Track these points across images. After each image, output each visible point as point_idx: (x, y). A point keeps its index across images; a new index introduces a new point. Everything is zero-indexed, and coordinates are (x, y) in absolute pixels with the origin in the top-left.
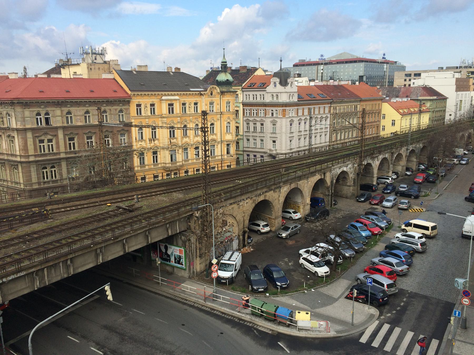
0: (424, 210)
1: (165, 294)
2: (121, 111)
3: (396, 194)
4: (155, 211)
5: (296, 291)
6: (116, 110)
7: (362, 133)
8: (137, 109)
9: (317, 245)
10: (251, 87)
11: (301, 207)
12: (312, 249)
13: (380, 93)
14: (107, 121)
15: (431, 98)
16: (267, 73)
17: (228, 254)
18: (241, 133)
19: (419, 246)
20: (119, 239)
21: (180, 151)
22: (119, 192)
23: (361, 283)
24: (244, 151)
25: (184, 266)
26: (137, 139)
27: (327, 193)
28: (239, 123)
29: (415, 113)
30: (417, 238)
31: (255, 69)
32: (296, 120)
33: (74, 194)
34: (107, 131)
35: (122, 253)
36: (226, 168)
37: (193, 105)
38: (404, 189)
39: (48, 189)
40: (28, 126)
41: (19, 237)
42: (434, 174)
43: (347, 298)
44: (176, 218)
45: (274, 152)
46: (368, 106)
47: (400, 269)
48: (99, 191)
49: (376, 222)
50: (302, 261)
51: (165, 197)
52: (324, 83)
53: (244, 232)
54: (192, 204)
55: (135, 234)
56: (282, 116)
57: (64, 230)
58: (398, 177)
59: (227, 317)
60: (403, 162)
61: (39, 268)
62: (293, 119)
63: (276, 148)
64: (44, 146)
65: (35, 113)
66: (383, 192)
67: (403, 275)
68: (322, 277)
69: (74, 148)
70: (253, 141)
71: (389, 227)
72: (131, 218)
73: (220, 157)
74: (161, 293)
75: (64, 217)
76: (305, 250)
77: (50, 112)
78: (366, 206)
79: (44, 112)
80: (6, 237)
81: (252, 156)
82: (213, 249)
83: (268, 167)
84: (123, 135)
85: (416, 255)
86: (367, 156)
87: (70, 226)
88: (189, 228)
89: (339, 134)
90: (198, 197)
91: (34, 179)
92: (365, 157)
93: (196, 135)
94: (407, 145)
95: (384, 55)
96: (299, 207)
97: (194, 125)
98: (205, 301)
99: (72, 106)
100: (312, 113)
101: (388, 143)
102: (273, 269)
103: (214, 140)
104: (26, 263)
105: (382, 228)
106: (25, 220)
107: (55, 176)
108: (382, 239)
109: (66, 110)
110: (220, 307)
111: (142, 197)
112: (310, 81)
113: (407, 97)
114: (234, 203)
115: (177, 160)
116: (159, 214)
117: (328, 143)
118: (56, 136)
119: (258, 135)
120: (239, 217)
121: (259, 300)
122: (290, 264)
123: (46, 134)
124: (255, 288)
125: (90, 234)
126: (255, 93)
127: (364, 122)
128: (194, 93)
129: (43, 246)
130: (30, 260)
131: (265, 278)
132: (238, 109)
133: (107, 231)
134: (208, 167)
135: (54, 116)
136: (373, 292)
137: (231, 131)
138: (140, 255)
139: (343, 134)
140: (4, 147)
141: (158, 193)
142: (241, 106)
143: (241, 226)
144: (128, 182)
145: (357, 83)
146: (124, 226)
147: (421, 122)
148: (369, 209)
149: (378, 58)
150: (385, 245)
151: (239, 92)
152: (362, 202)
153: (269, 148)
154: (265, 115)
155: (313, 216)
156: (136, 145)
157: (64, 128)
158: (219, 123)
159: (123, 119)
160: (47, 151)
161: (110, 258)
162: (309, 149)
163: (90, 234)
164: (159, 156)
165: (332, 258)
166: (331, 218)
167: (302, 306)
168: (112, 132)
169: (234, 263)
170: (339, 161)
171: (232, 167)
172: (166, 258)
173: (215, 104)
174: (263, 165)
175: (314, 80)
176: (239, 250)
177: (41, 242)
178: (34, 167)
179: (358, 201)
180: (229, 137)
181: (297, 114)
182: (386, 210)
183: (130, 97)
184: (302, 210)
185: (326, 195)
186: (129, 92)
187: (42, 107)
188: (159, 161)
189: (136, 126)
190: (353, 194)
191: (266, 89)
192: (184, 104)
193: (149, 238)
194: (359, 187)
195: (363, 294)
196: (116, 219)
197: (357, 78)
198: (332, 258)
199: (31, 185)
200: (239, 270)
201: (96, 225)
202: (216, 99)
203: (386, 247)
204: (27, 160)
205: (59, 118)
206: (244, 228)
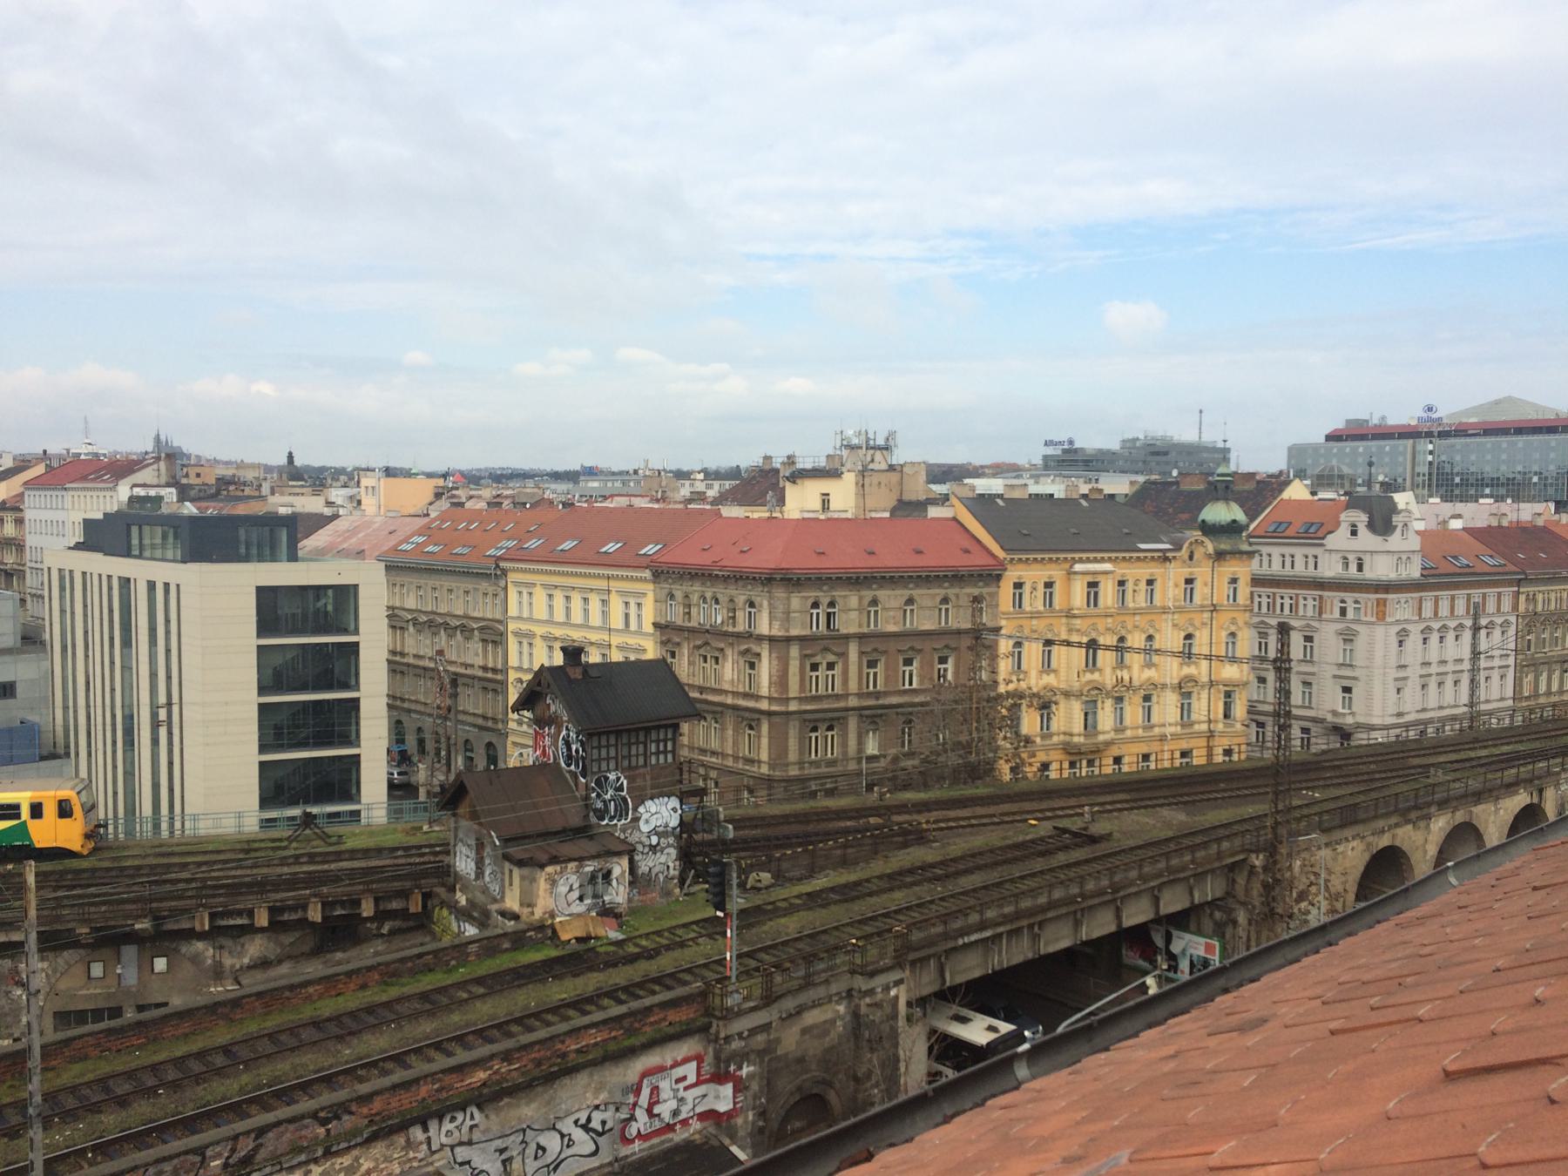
21: (1109, 703)
37: (1143, 586)
40: (794, 632)
45: (1349, 720)
56: (1374, 619)
62: (1409, 627)
63: (1354, 709)
65: (810, 602)
73: (1204, 727)
77: (838, 599)
89: (1545, 675)
91: (793, 756)
97: (1144, 637)
99: (881, 587)
109: (868, 595)
115: (1100, 727)
118: (843, 655)
123: (826, 649)
126: (1287, 550)
153: (1328, 707)
154: (1320, 614)
157: (861, 637)
181: (1420, 615)
187: (825, 588)
202: (1202, 572)
204: (783, 709)
205: (854, 615)
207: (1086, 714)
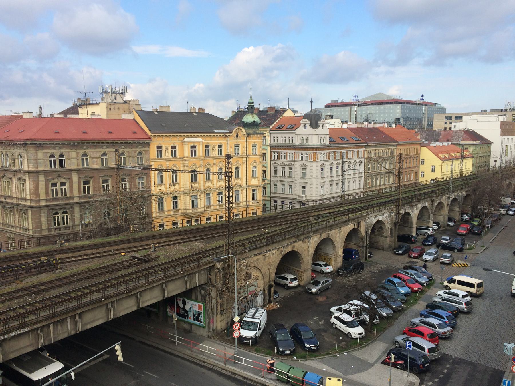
0: (469, 265)
1: (181, 355)
2: (140, 153)
3: (438, 247)
4: (173, 261)
5: (327, 354)
6: (135, 152)
7: (399, 179)
8: (157, 151)
9: (350, 302)
10: (280, 128)
11: (333, 259)
12: (345, 307)
13: (419, 137)
14: (124, 163)
15: (474, 142)
16: (297, 115)
17: (252, 311)
18: (268, 177)
19: (464, 306)
20: (133, 293)
21: (202, 196)
22: (135, 240)
23: (400, 346)
24: (271, 197)
25: (203, 324)
26: (157, 183)
27: (361, 245)
28: (266, 167)
29: (456, 158)
30: (461, 296)
31: (284, 110)
32: (327, 164)
33: (87, 242)
34: (124, 174)
35: (135, 308)
36: (251, 215)
37: (217, 148)
38: (446, 242)
39: (58, 236)
40: (41, 169)
41: (25, 289)
42: (479, 225)
43: (383, 363)
44: (196, 270)
45: (304, 198)
46: (405, 150)
47: (442, 331)
48: (113, 238)
49: (416, 278)
50: (333, 320)
51: (184, 246)
52: (359, 125)
53: (270, 287)
54: (213, 254)
55: (150, 287)
56: (312, 160)
57: (73, 282)
58: (439, 228)
59: (250, 382)
60: (445, 211)
61: (44, 323)
62: (324, 163)
64: (56, 190)
65: (49, 155)
66: (423, 244)
67: (447, 338)
68: (356, 339)
69: (89, 192)
70: (281, 187)
71: (430, 283)
72: (147, 270)
73: (245, 204)
74: (177, 353)
75: (75, 267)
76: (337, 307)
77: (64, 154)
78: (405, 260)
79: (59, 154)
80: (10, 288)
81: (279, 203)
82: (236, 304)
83: (297, 215)
84: (141, 178)
85: (461, 315)
86: (405, 204)
87: (80, 277)
88: (209, 281)
89: (375, 179)
90: (220, 247)
92: (403, 205)
93: (220, 180)
94: (449, 193)
95: (422, 96)
96: (330, 259)
97: (218, 168)
98: (225, 364)
99: (88, 148)
100: (345, 157)
101: (427, 190)
102: (301, 328)
103: (238, 185)
104: (31, 317)
105: (422, 285)
106: (32, 270)
107: (67, 223)
108: (422, 296)
109: (81, 151)
110: (242, 371)
111: (159, 247)
112: (343, 122)
113: (448, 141)
114: (259, 254)
116: (178, 265)
117: (362, 190)
118: (70, 179)
119: (286, 179)
120: (265, 270)
121: (285, 363)
122: (320, 323)
123: (59, 177)
124: (281, 349)
125: (101, 286)
126: (283, 135)
127: (401, 168)
128: (218, 134)
129: (50, 299)
130: (35, 314)
131: (292, 338)
132: (265, 152)
133: (120, 284)
134: (232, 214)
135: (69, 158)
136: (412, 357)
137: (257, 176)
138: (155, 310)
139: (378, 180)
140: (14, 191)
141: (177, 242)
142: (269, 148)
143: (267, 280)
144: (145, 229)
145: (394, 126)
146: (138, 278)
147: (464, 168)
148: (408, 262)
149: (416, 98)
150: (426, 304)
151: (267, 134)
152: (400, 254)
153: (298, 194)
154: (294, 159)
155: (345, 270)
156: (155, 190)
157: (78, 171)
158: (244, 166)
159: (142, 161)
160: (59, 195)
161: (122, 314)
162: (342, 196)
163: (101, 286)
164: (179, 202)
165: (367, 318)
166: (366, 273)
167: (333, 371)
168: (129, 175)
169: (258, 321)
170: (375, 209)
171: (258, 214)
172: (183, 314)
173: (240, 147)
174: (292, 213)
175: (346, 122)
176: (264, 306)
177: (48, 295)
178: (44, 213)
179: (395, 254)
180: (255, 182)
181: (329, 158)
182: (428, 264)
183: (150, 138)
184: (333, 263)
185: (360, 247)
186: (149, 133)
187: (57, 148)
188: (179, 207)
189: (155, 170)
190: (390, 246)
191: (295, 131)
192: (207, 146)
193: (166, 292)
194: (397, 238)
195: (402, 359)
196: (130, 270)
197: (393, 120)
198: (367, 318)
200: (264, 329)
201: (108, 276)
202: (242, 142)
203: (428, 306)
204: (37, 204)
205: (74, 161)
206: (270, 282)
207: (193, 201)
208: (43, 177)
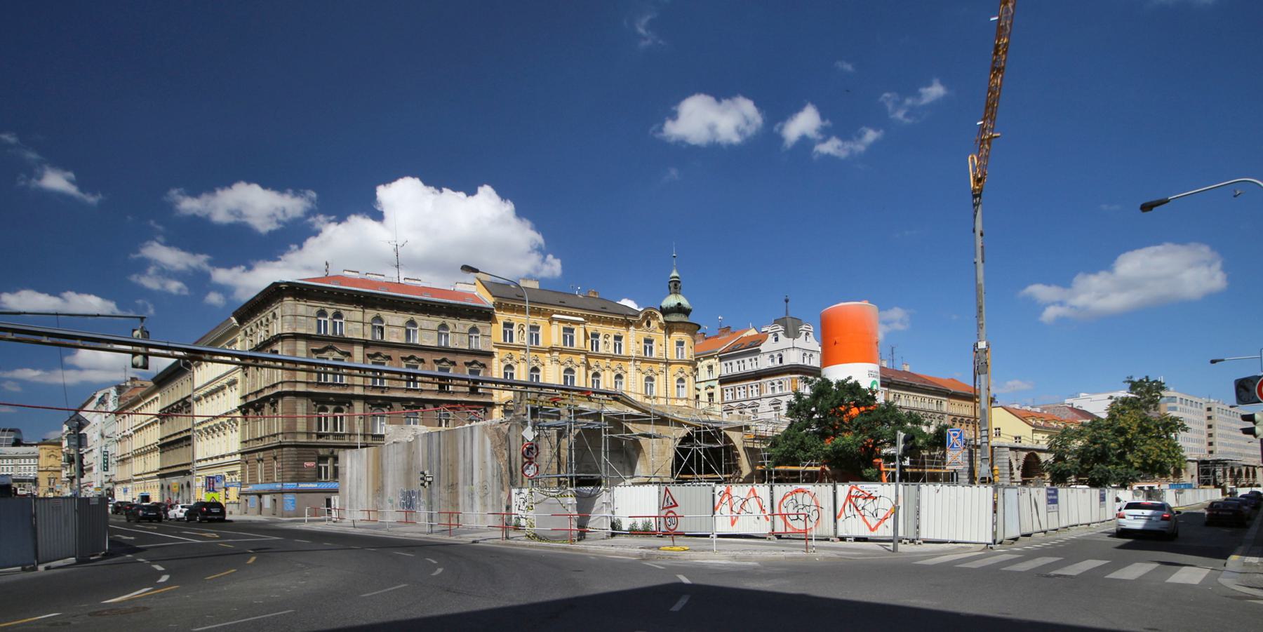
2: (474, 330)
37: (611, 340)
91: (301, 425)
109: (371, 314)
157: (366, 344)
178: (302, 404)
199: (295, 433)
202: (659, 336)
204: (292, 389)
208: (305, 346)
